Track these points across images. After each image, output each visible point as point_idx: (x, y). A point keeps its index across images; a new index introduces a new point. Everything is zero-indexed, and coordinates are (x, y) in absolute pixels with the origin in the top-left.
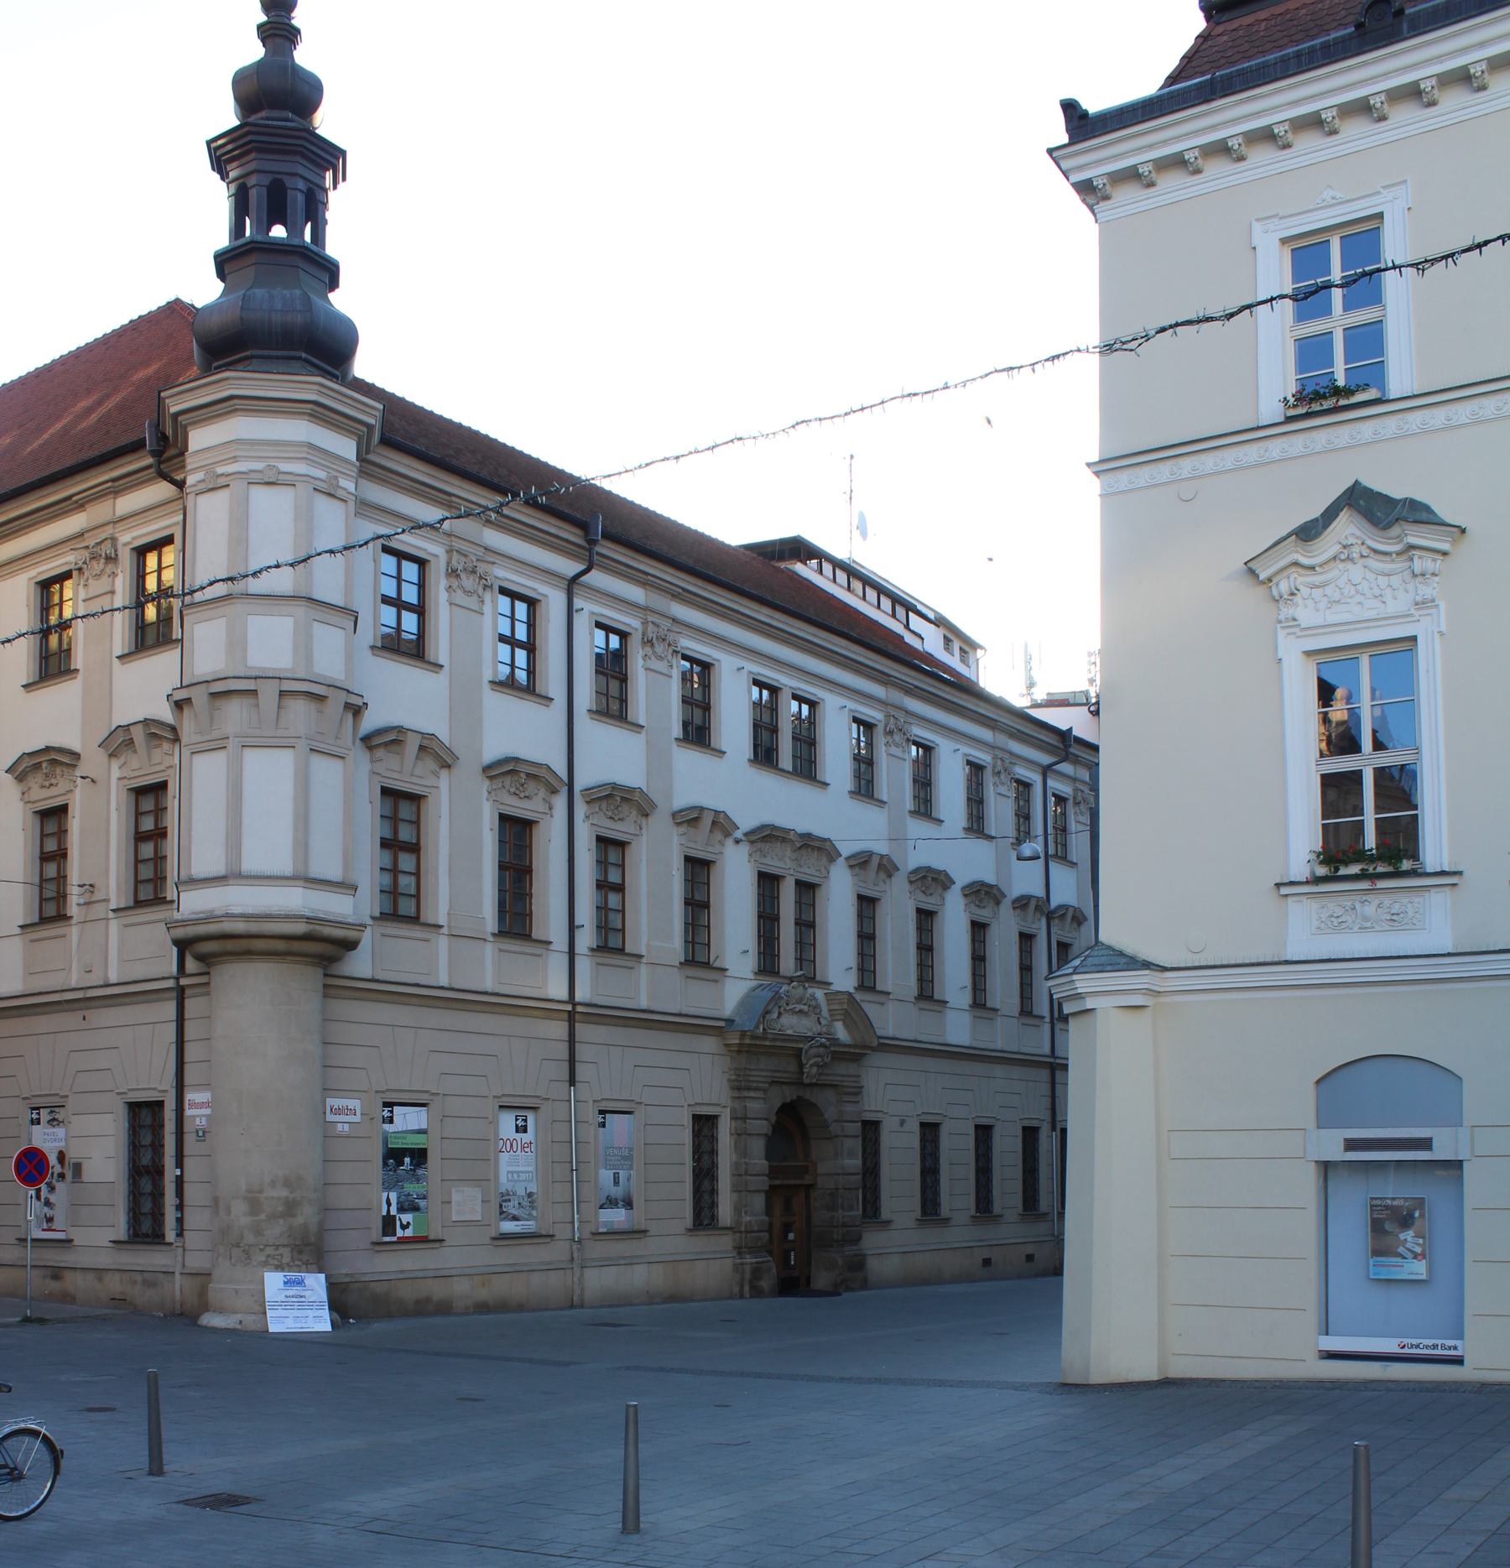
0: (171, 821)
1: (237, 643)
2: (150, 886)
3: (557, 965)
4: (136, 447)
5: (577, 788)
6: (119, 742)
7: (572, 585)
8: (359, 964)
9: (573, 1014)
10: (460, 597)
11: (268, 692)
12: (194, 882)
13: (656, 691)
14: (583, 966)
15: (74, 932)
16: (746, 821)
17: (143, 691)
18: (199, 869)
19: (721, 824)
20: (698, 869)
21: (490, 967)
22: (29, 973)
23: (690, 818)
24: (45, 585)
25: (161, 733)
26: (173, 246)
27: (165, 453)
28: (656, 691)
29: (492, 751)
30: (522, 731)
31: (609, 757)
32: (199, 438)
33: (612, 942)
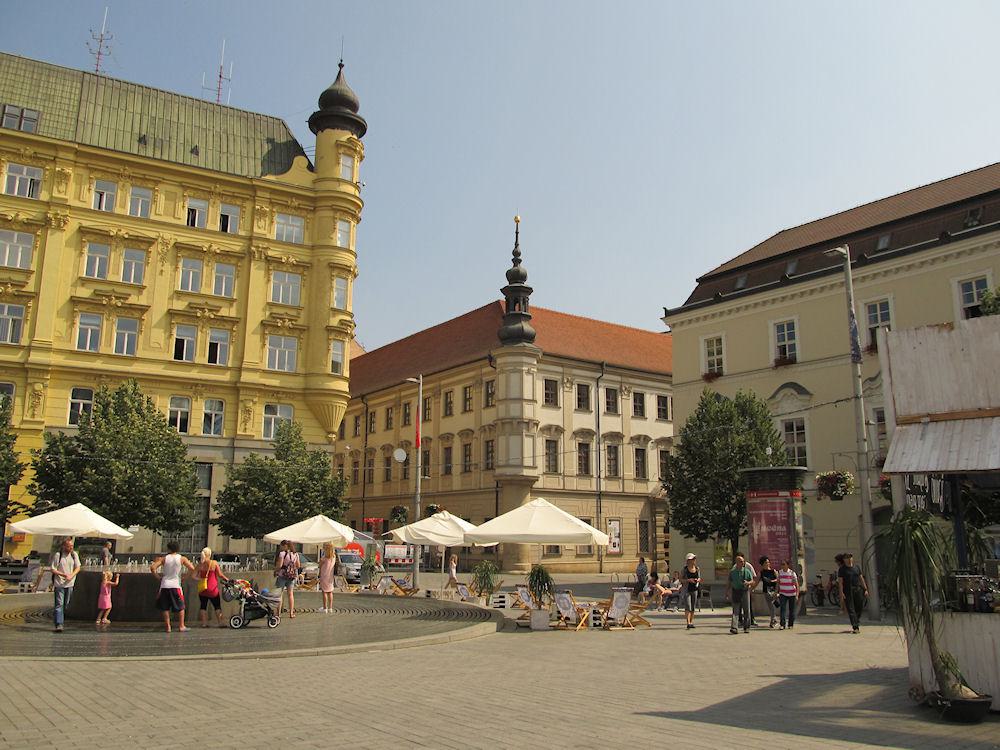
0: (494, 449)
1: (507, 411)
2: (490, 467)
3: (594, 480)
4: (485, 358)
5: (601, 433)
6: (483, 429)
7: (598, 380)
8: (538, 485)
9: (600, 495)
10: (566, 389)
11: (515, 422)
12: (499, 467)
13: (626, 404)
14: (603, 482)
15: (473, 475)
16: (654, 436)
17: (489, 416)
18: (501, 463)
19: (646, 439)
20: (641, 454)
21: (575, 484)
22: (462, 484)
23: (636, 439)
24: (466, 388)
25: (492, 427)
26: (492, 291)
27: (491, 359)
28: (626, 404)
29: (576, 427)
30: (586, 421)
31: (610, 424)
32: (499, 361)
33: (614, 472)
